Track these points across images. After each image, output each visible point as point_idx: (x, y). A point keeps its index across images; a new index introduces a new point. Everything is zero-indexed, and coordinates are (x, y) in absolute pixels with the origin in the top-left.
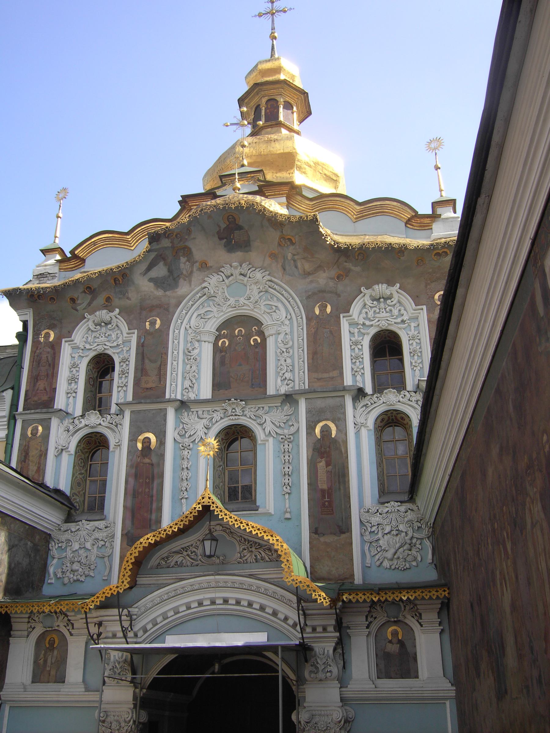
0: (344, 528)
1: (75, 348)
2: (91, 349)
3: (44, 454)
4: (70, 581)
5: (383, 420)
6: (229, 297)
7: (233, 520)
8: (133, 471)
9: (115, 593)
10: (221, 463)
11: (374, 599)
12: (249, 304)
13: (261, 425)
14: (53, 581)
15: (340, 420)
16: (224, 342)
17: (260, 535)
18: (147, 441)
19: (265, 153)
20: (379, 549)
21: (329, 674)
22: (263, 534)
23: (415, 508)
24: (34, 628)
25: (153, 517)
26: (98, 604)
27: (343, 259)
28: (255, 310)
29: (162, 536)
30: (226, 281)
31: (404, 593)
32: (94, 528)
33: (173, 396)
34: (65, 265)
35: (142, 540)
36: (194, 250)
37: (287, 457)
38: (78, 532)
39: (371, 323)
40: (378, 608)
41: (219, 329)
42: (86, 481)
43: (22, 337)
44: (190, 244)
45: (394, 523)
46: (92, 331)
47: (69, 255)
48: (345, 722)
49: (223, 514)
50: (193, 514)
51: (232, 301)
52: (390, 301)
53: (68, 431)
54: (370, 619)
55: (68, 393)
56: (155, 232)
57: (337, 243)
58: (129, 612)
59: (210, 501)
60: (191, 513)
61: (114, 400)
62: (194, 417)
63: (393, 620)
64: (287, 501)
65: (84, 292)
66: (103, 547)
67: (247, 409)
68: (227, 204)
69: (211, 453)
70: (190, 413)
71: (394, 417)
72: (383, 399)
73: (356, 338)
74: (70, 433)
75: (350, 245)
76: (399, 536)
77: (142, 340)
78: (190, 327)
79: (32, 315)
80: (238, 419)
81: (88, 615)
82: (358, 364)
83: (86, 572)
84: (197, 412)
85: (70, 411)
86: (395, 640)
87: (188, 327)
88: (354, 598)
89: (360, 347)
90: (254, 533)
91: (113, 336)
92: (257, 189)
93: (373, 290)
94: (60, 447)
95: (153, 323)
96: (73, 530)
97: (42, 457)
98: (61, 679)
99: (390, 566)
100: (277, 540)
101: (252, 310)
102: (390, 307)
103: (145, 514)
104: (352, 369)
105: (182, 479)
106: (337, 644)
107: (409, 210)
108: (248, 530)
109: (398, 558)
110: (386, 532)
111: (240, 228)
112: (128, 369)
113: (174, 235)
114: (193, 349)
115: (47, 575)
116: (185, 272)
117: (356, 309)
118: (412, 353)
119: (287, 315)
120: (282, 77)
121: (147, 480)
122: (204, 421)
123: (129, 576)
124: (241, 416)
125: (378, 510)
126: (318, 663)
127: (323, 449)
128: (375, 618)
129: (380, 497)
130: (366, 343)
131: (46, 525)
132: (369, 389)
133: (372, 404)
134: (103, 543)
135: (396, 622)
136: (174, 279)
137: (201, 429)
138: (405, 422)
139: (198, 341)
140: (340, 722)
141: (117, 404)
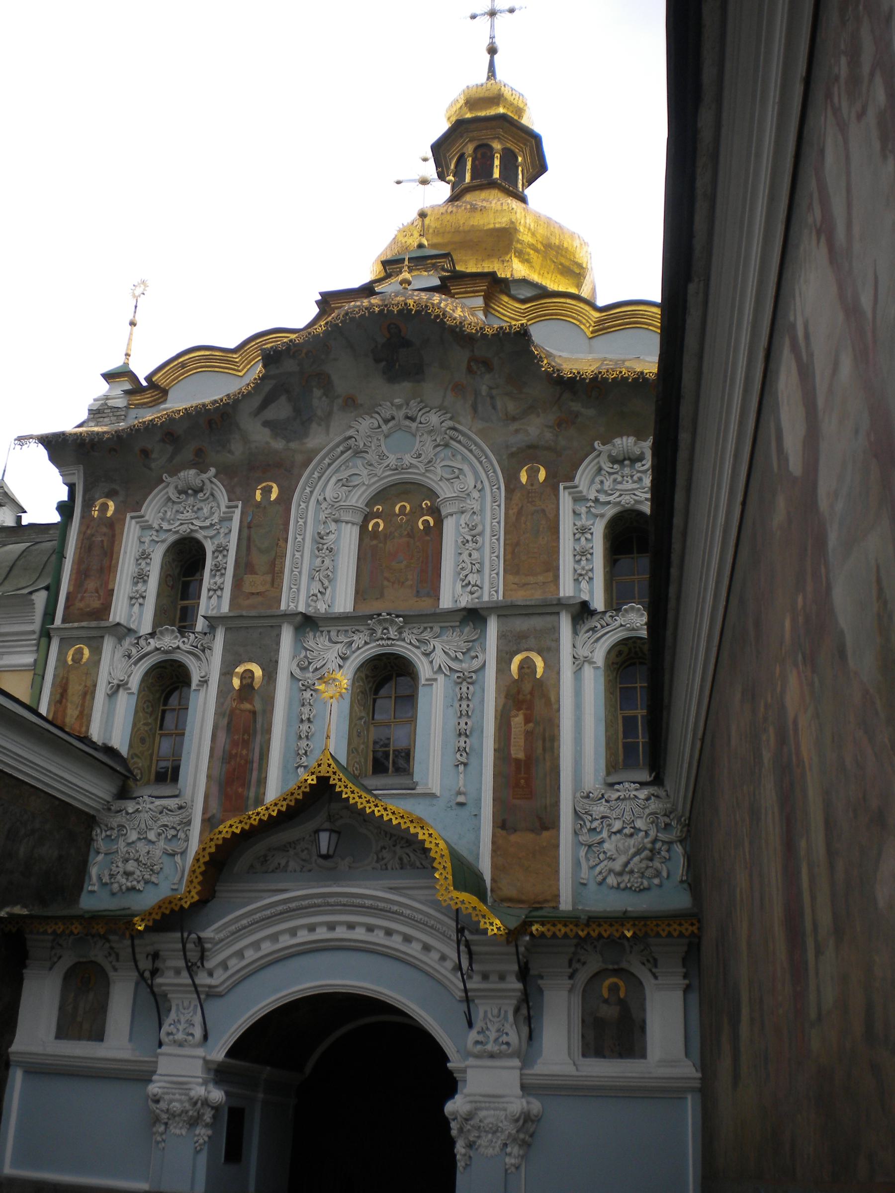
0: (548, 822)
1: (146, 527)
2: (170, 530)
3: (89, 693)
5: (620, 653)
6: (386, 452)
7: (364, 800)
8: (225, 721)
9: (177, 909)
10: (363, 714)
11: (581, 933)
12: (418, 464)
13: (427, 655)
14: (96, 888)
15: (551, 653)
16: (377, 524)
17: (403, 826)
19: (466, 228)
20: (602, 856)
21: (504, 1047)
22: (409, 824)
23: (662, 793)
24: (60, 957)
25: (252, 794)
26: (150, 924)
28: (427, 474)
29: (254, 823)
30: (384, 427)
31: (628, 925)
32: (160, 808)
33: (292, 605)
34: (137, 399)
35: (221, 827)
37: (464, 706)
38: (137, 815)
41: (370, 503)
42: (154, 735)
43: (65, 509)
46: (174, 502)
47: (144, 384)
48: (525, 1122)
49: (348, 790)
50: (303, 789)
51: (392, 460)
52: (638, 465)
53: (129, 657)
54: (576, 965)
55: (131, 598)
56: (272, 347)
57: (558, 370)
58: (199, 938)
60: (299, 788)
61: (202, 611)
62: (323, 641)
63: (611, 967)
64: (462, 776)
65: (163, 440)
67: (407, 630)
68: (386, 306)
70: (318, 634)
71: (638, 649)
72: (620, 620)
73: (584, 521)
74: (133, 660)
75: (579, 373)
76: (635, 837)
77: (249, 519)
78: (325, 499)
79: (82, 475)
80: (392, 645)
81: (137, 942)
82: (583, 563)
83: (147, 877)
84: (329, 632)
85: (133, 626)
87: (321, 498)
88: (548, 930)
89: (589, 536)
90: (395, 822)
91: (205, 510)
92: (437, 282)
93: (614, 445)
94: (116, 682)
95: (267, 491)
96: (130, 811)
97: (88, 697)
98: (98, 1036)
99: (619, 884)
100: (430, 835)
101: (423, 475)
102: (639, 475)
103: (240, 790)
104: (575, 570)
105: (300, 736)
108: (386, 818)
109: (632, 872)
110: (614, 830)
112: (226, 563)
113: (303, 355)
114: (328, 534)
115: (87, 878)
116: (319, 413)
117: (584, 476)
119: (476, 482)
120: (501, 110)
121: (246, 737)
122: (339, 646)
123: (199, 883)
124: (397, 640)
125: (603, 795)
126: (488, 1029)
128: (584, 964)
129: (608, 773)
130: (599, 530)
131: (87, 801)
132: (598, 604)
133: (603, 627)
134: (173, 832)
135: (618, 972)
137: (333, 659)
139: (336, 521)
140: (517, 1120)
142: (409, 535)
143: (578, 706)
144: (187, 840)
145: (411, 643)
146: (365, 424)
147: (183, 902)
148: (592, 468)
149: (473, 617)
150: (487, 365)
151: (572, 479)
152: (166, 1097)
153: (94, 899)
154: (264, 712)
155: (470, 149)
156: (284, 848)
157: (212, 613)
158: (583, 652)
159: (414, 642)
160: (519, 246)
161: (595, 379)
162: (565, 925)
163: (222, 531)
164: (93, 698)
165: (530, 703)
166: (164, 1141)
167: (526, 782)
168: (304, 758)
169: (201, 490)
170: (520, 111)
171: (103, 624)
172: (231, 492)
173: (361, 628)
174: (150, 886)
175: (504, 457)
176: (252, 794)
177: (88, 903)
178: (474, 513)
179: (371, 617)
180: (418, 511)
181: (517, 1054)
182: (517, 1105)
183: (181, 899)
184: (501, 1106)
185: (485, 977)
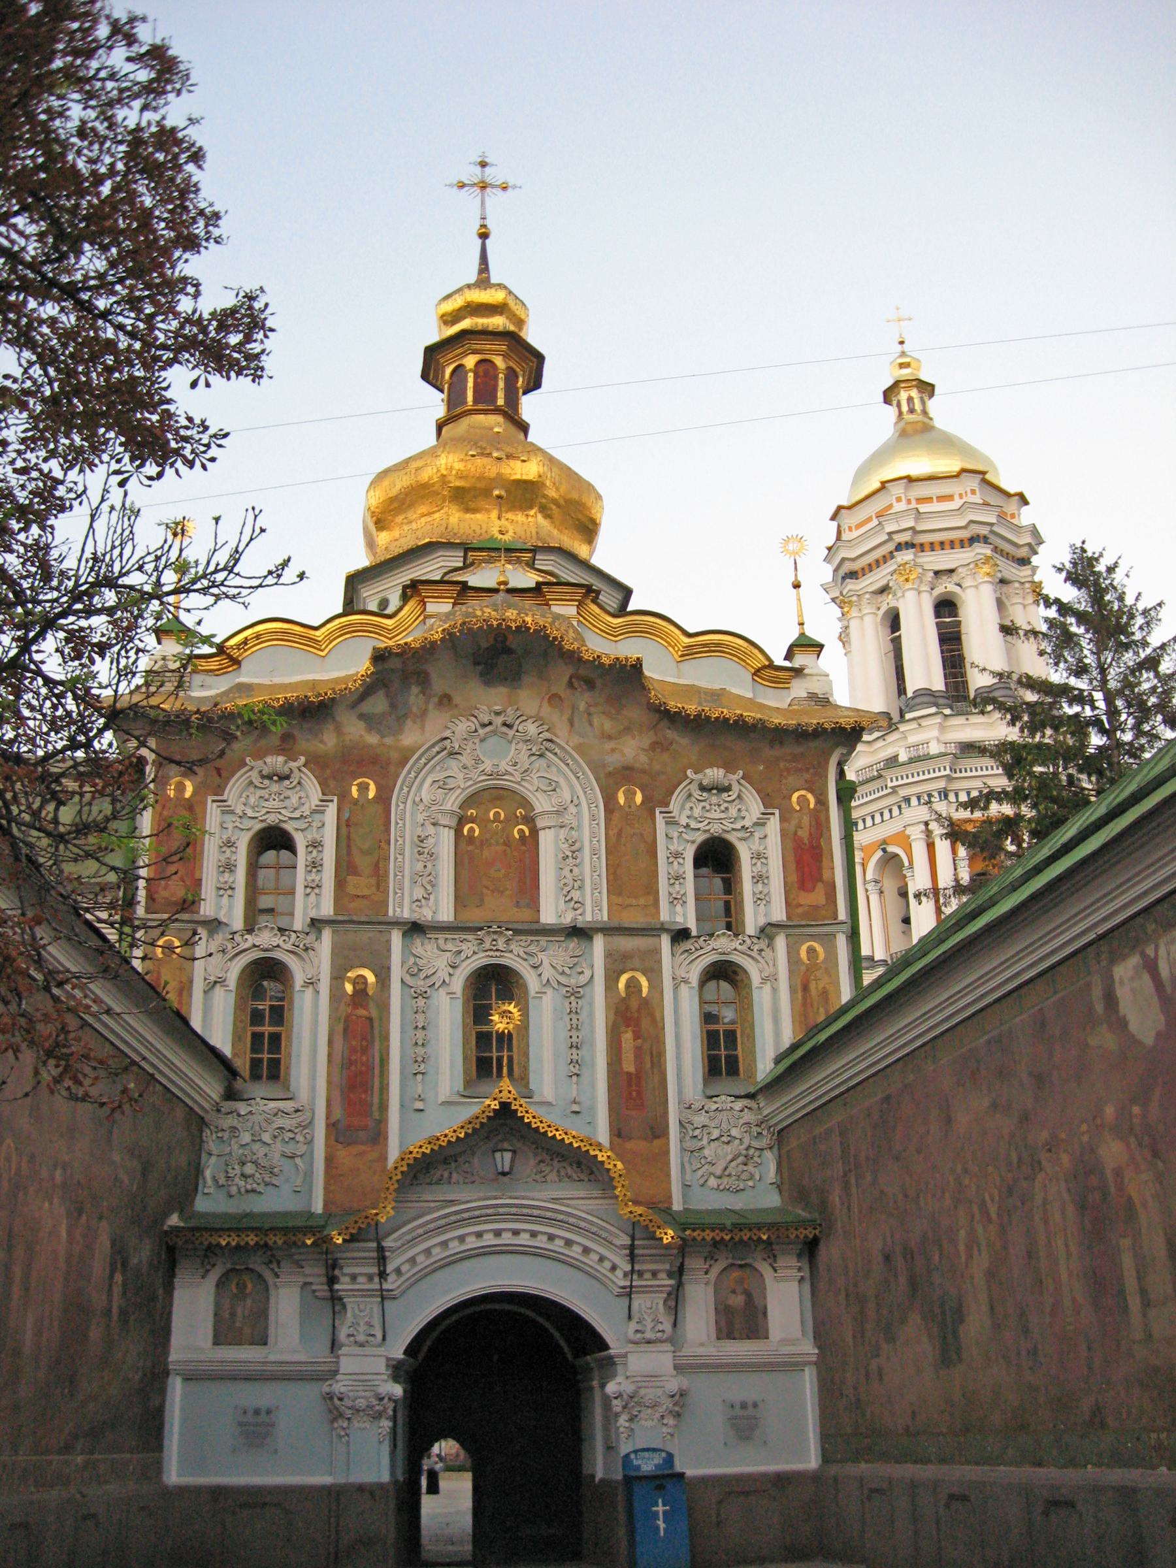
0: (658, 1131)
3: (186, 987)
4: (239, 1192)
8: (341, 1026)
9: (373, 1223)
14: (211, 1190)
15: (654, 973)
16: (471, 830)
18: (360, 981)
20: (703, 1161)
21: (659, 1335)
24: (214, 1265)
25: (376, 1100)
26: (347, 1237)
27: (665, 723)
28: (523, 783)
31: (764, 1230)
36: (434, 677)
37: (574, 1021)
39: (700, 825)
40: (723, 1248)
44: (428, 667)
45: (724, 1126)
51: (487, 766)
52: (726, 794)
53: (223, 951)
58: (383, 1248)
59: (511, 1096)
66: (292, 1142)
69: (511, 1026)
72: (713, 944)
77: (347, 815)
82: (677, 887)
85: (224, 920)
86: (739, 1290)
89: (681, 861)
90: (575, 1145)
94: (213, 979)
95: (364, 788)
97: (185, 993)
101: (518, 783)
102: (726, 805)
104: (670, 894)
106: (669, 1294)
107: (760, 656)
108: (567, 1142)
109: (729, 1175)
111: (508, 651)
115: (201, 1181)
116: (415, 709)
118: (759, 878)
121: (364, 1043)
122: (448, 954)
127: (629, 1014)
131: (206, 1105)
134: (291, 1135)
136: (398, 719)
138: (738, 978)
139: (434, 824)
140: (673, 1396)
141: (312, 919)
142: (507, 844)
143: (677, 1023)
144: (310, 1142)
145: (519, 956)
146: (463, 727)
147: (379, 1217)
148: (684, 795)
149: (579, 933)
150: (590, 684)
151: (667, 805)
152: (351, 1394)
153: (209, 1202)
154: (381, 1019)
155: (470, 361)
156: (446, 1161)
157: (313, 914)
158: (681, 973)
159: (522, 954)
160: (544, 501)
161: (698, 716)
162: (713, 1230)
163: (314, 824)
164: (190, 995)
165: (634, 1018)
166: (347, 1435)
167: (636, 1092)
168: (423, 1066)
169: (287, 777)
170: (520, 323)
171: (196, 917)
172: (324, 784)
173: (470, 937)
174: (270, 1188)
175: (602, 775)
176: (376, 1100)
177: (201, 1205)
178: (572, 828)
179: (481, 929)
180: (512, 820)
181: (671, 1340)
182: (673, 1385)
183: (377, 1214)
184: (658, 1384)
185: (641, 1274)
